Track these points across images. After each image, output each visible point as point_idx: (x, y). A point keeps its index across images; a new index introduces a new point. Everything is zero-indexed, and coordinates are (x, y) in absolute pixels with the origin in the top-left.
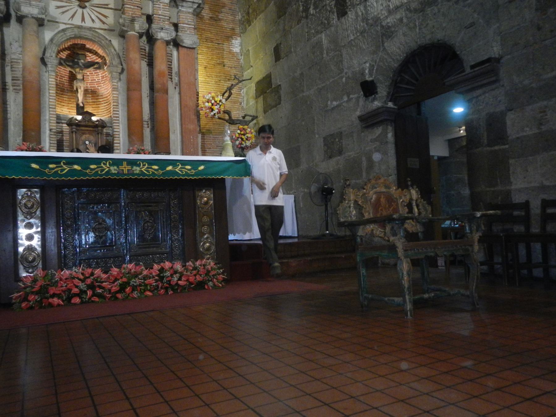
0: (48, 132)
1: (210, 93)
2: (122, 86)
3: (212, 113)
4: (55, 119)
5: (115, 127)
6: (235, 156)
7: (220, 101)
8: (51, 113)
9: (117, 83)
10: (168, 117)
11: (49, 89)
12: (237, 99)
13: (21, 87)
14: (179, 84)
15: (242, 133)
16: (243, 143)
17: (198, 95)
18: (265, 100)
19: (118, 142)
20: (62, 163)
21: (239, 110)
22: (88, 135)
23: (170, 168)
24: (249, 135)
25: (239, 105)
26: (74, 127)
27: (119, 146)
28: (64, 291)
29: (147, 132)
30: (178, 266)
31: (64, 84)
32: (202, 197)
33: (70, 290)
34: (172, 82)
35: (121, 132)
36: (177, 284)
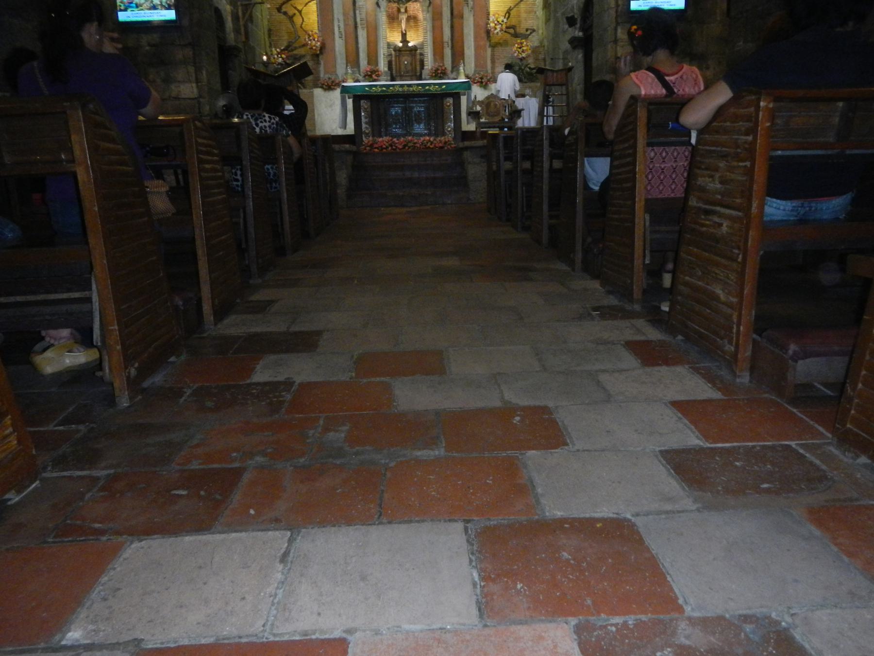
0: (382, 56)
1: (494, 15)
2: (429, 16)
3: (496, 32)
4: (386, 46)
5: (425, 49)
6: (466, 79)
7: (503, 21)
8: (384, 42)
9: (426, 14)
10: (463, 37)
11: (382, 25)
12: (531, 9)
13: (365, 26)
14: (472, 8)
15: (519, 46)
16: (520, 55)
17: (489, 15)
18: (546, 12)
19: (427, 60)
20: (378, 87)
21: (533, 19)
22: (406, 57)
23: (427, 88)
24: (524, 48)
25: (533, 14)
26: (397, 52)
27: (428, 63)
28: (380, 147)
29: (448, 52)
30: (432, 139)
31: (394, 14)
32: (447, 102)
33: (382, 146)
34: (468, 6)
35: (429, 52)
36: (429, 147)
